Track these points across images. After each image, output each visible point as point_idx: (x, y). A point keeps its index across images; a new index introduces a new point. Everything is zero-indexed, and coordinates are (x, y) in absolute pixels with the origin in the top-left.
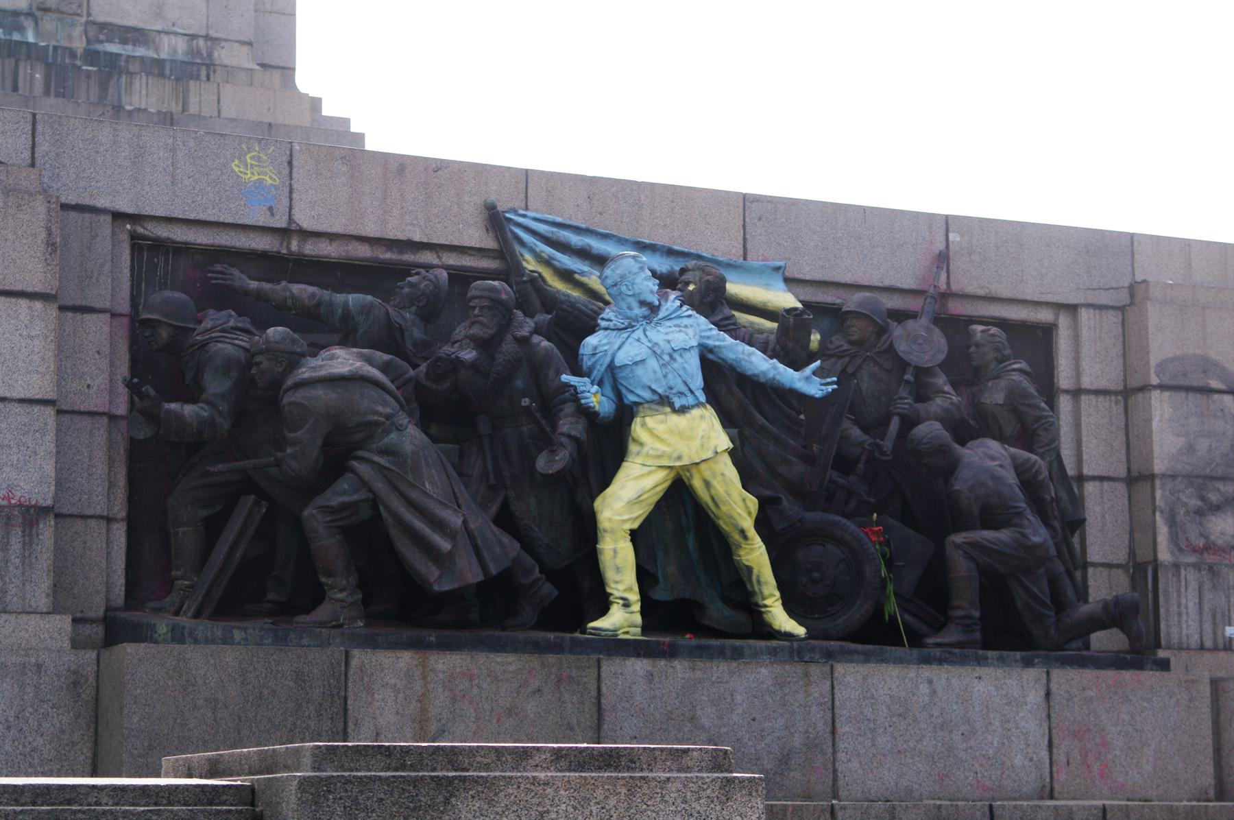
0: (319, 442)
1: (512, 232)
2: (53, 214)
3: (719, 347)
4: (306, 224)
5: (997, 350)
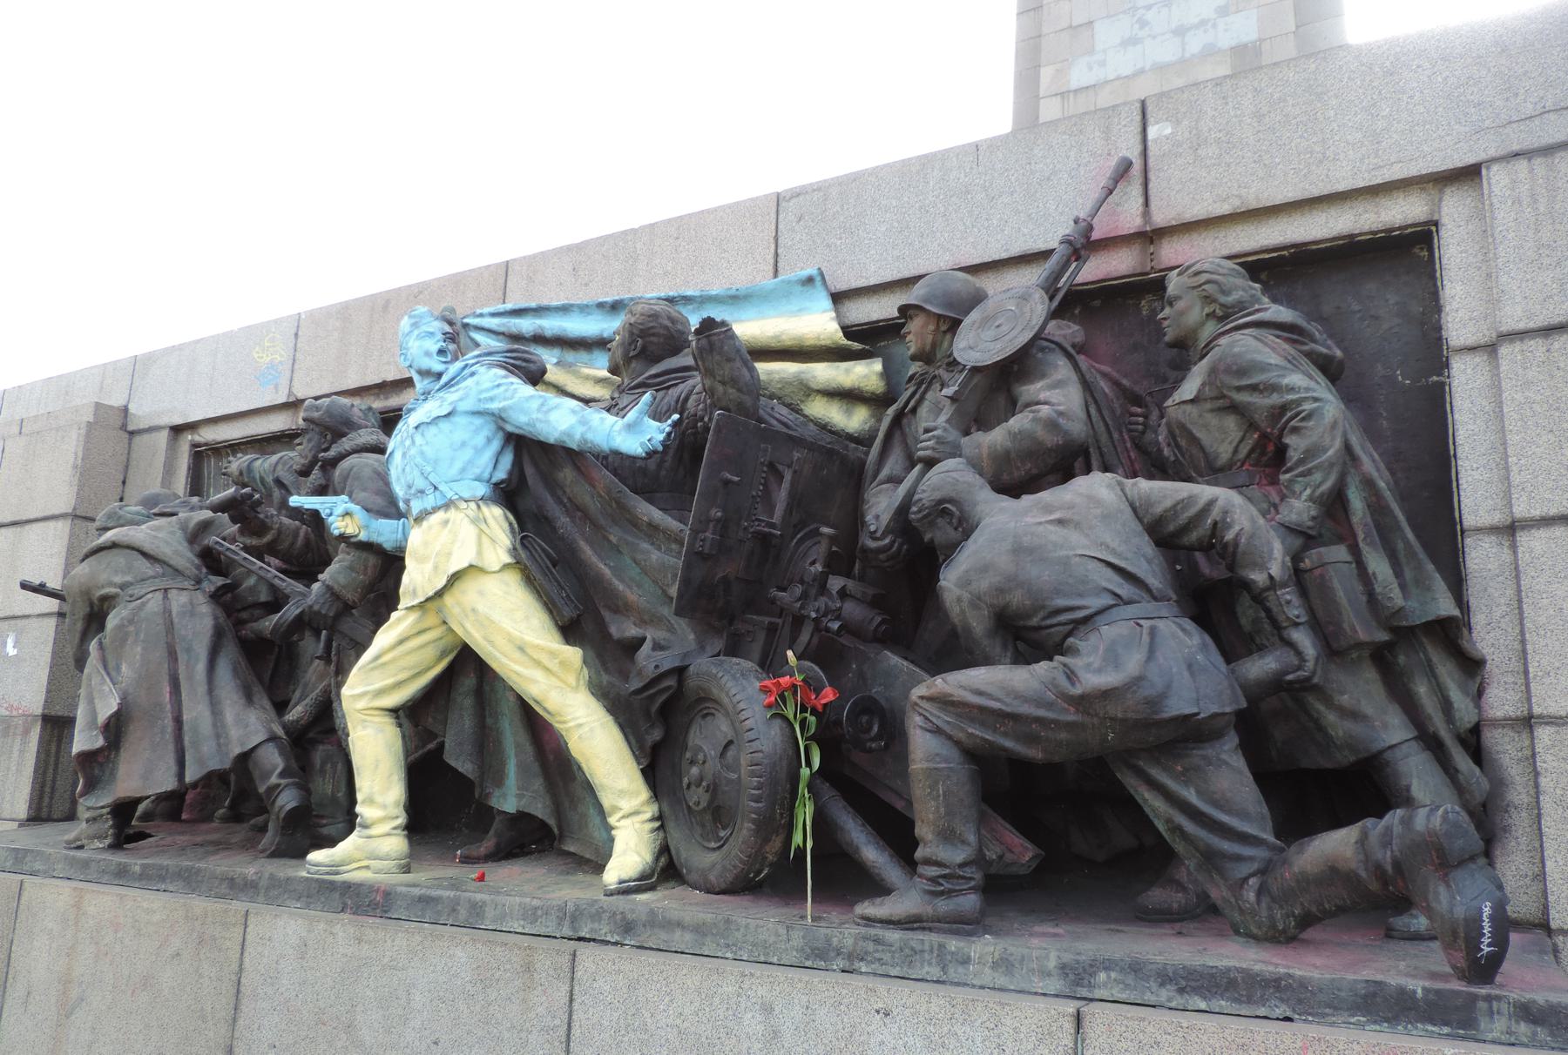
3: (503, 409)
5: (1208, 299)
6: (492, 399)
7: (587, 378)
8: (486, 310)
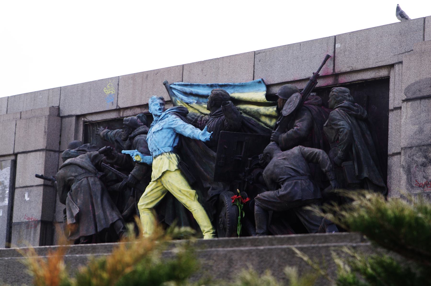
0: (61, 189)
3: (175, 128)
6: (172, 124)
8: (177, 83)
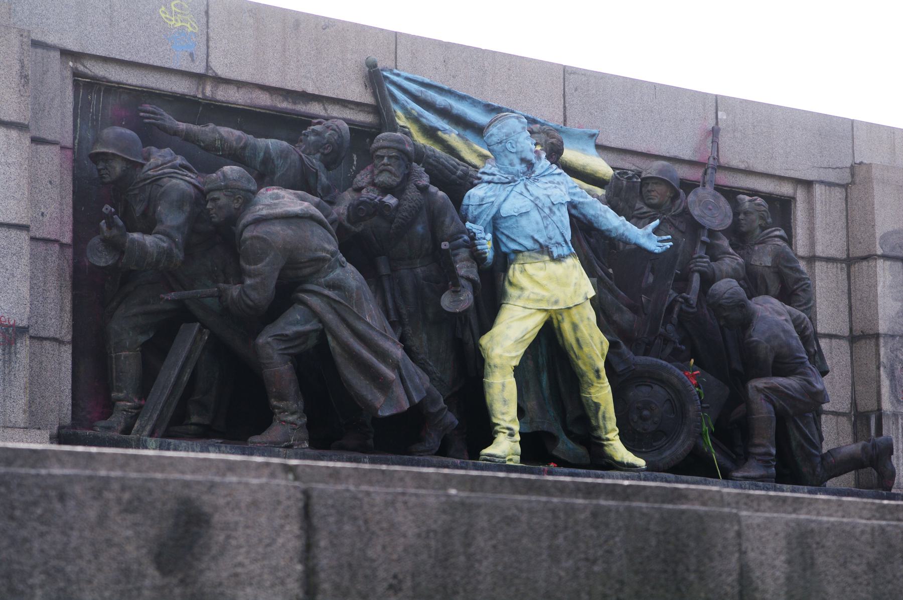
0: (276, 274)
1: (389, 90)
2: (26, 48)
3: (582, 203)
4: (222, 72)
5: (762, 218)
7: (475, 151)
